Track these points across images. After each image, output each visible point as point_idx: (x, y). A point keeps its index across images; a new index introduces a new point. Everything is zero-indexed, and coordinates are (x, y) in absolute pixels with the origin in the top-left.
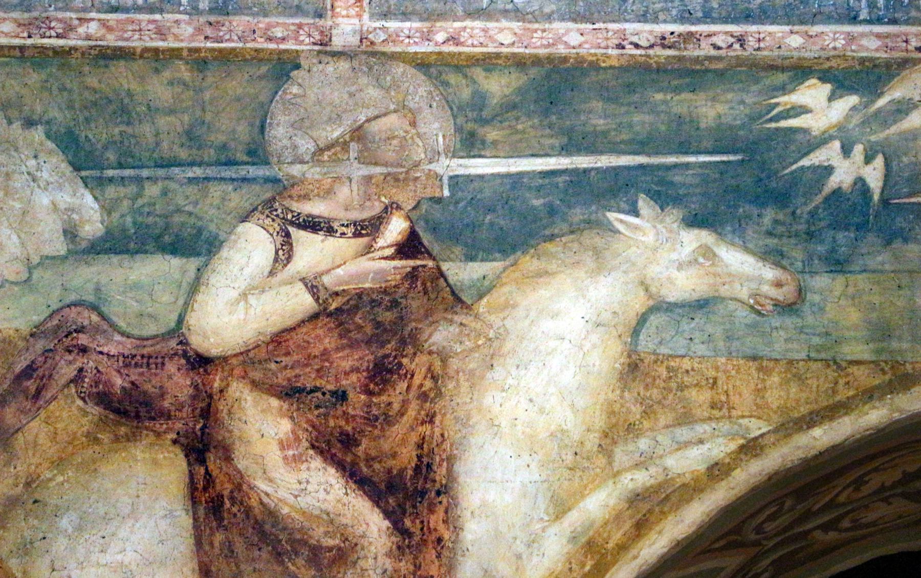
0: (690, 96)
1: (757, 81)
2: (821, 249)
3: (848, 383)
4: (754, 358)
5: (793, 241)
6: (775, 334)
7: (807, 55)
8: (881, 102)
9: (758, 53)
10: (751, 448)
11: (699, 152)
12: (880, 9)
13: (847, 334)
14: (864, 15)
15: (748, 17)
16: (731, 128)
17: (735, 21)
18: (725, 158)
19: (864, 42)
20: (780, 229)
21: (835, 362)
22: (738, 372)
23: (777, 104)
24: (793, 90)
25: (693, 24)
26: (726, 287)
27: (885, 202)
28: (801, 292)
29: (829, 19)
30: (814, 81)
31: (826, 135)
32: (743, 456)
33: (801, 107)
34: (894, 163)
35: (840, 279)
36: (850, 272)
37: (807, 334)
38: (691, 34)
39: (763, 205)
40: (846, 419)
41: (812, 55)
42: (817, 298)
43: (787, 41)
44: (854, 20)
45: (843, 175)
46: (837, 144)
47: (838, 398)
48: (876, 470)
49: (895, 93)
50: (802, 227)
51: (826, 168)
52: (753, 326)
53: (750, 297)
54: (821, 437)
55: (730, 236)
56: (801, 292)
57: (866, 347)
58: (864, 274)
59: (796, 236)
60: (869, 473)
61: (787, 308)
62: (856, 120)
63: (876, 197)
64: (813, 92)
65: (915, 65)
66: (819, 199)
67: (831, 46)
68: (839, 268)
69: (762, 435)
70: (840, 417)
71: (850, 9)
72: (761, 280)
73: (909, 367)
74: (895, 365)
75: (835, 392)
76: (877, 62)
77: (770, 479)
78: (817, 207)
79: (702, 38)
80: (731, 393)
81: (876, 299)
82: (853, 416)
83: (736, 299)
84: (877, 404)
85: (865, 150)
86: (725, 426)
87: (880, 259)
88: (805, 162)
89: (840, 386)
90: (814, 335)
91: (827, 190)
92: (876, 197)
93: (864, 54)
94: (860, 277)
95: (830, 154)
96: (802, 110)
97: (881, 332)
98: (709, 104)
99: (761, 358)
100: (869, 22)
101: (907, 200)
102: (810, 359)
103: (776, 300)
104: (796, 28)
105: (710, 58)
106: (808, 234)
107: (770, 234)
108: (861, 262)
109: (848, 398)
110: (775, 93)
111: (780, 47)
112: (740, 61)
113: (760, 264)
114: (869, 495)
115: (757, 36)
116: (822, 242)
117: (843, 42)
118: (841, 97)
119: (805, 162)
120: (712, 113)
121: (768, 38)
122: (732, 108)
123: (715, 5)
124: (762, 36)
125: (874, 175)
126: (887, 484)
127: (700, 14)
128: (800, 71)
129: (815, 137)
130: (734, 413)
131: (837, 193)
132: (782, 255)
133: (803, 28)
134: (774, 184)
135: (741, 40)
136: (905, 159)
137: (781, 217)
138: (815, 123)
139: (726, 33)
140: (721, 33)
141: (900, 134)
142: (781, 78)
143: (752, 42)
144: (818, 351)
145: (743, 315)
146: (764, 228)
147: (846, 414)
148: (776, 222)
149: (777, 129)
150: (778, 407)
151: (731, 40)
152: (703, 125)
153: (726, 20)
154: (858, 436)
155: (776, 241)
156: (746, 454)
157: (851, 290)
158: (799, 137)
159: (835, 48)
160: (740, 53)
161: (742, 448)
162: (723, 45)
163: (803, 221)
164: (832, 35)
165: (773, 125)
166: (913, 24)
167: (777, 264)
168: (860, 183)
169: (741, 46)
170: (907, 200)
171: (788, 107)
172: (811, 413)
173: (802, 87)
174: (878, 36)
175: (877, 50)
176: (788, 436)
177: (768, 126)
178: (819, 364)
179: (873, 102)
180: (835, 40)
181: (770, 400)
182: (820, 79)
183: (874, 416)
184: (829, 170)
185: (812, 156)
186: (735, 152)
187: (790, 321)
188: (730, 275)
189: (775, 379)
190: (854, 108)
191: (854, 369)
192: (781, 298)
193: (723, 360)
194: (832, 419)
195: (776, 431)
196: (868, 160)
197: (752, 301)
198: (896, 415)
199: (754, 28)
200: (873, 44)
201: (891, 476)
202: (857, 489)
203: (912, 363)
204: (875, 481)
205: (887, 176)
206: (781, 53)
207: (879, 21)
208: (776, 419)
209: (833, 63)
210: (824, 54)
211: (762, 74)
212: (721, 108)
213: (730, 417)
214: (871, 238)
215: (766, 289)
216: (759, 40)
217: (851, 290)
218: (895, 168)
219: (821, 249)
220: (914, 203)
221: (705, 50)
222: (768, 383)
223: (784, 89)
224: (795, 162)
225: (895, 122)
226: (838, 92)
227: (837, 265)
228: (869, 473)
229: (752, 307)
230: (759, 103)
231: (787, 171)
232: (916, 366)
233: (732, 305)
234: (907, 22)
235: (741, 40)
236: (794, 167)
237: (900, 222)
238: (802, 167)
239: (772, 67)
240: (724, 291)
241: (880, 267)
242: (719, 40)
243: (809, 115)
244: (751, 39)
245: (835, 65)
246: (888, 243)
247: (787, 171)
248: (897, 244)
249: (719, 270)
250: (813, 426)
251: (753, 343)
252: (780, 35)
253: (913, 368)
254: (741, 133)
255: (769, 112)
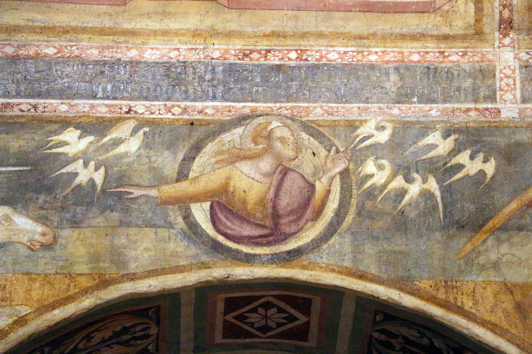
0: (6, 136)
1: (42, 128)
2: (68, 216)
3: (75, 285)
4: (27, 274)
5: (53, 211)
6: (39, 260)
7: (68, 115)
8: (106, 140)
9: (44, 114)
10: (21, 321)
11: (8, 165)
12: (108, 92)
13: (78, 260)
14: (100, 95)
15: (39, 95)
16: (26, 152)
17: (32, 97)
18: (21, 168)
19: (99, 109)
20: (47, 205)
21: (70, 275)
22: (18, 281)
23: (52, 141)
24: (60, 134)
25: (10, 98)
26: (16, 236)
27: (103, 191)
28: (55, 239)
29: (82, 97)
30: (72, 128)
31: (76, 157)
32: (15, 326)
33: (64, 142)
34: (110, 171)
35: (77, 231)
36: (82, 227)
37: (57, 260)
38: (9, 104)
39: (41, 193)
40: (73, 304)
41: (71, 115)
42: (63, 241)
43: (59, 108)
44: (95, 97)
45: (83, 178)
46: (81, 161)
47: (69, 294)
48: (96, 330)
49: (114, 134)
50: (59, 204)
51: (74, 173)
52: (29, 256)
53: (28, 241)
54: (59, 314)
55: (20, 210)
56: (55, 239)
57: (87, 266)
58: (89, 229)
59: (55, 209)
60: (93, 332)
61: (47, 247)
62: (91, 149)
63: (99, 189)
64: (71, 134)
65: (124, 120)
66: (70, 189)
67: (82, 111)
68: (76, 225)
69: (27, 315)
70: (69, 303)
71: (93, 91)
72: (34, 233)
73: (107, 276)
74: (101, 275)
75: (68, 290)
76: (105, 119)
77: (29, 337)
78: (68, 194)
79: (14, 106)
80: (12, 293)
81: (94, 241)
82: (76, 303)
83: (20, 243)
84: (89, 296)
85: (96, 164)
86: (7, 310)
87: (98, 220)
88: (64, 171)
89: (71, 288)
90: (60, 260)
91: (73, 185)
92: (99, 189)
93: (99, 115)
94: (86, 230)
95: (77, 166)
96: (65, 143)
97: (95, 258)
98: (15, 140)
99: (31, 274)
100: (102, 98)
101: (114, 190)
102: (57, 273)
103: (42, 243)
104: (65, 101)
105: (18, 117)
106: (61, 208)
107: (42, 208)
108: (88, 222)
109: (75, 294)
110: (51, 135)
111: (55, 111)
112: (34, 118)
113: (35, 224)
114: (99, 343)
115: (44, 105)
116: (68, 212)
117: (88, 109)
118: (85, 137)
119: (64, 171)
120: (16, 145)
121: (49, 106)
122: (28, 143)
123: (23, 89)
124: (46, 105)
125: (99, 177)
126: (106, 337)
127: (14, 93)
128: (65, 123)
129: (70, 158)
130: (13, 303)
131: (79, 186)
132: (47, 219)
133: (69, 101)
134: (46, 182)
135: (35, 107)
136: (115, 169)
137: (48, 199)
138: (70, 150)
139: (27, 103)
140: (25, 103)
141: (114, 156)
142: (55, 127)
143: (41, 108)
144: (62, 269)
145: (24, 251)
146: (38, 206)
147: (73, 302)
148: (45, 202)
149: (50, 154)
150: (37, 300)
151: (30, 107)
152: (11, 152)
153: (27, 97)
154: (78, 313)
155: (45, 212)
156: (17, 325)
157: (82, 237)
158: (62, 157)
159: (84, 112)
160: (33, 114)
161: (15, 322)
162: (26, 110)
163: (59, 201)
164: (83, 105)
165: (49, 151)
166: (125, 100)
167: (44, 224)
168: (92, 181)
169: (35, 110)
170: (114, 190)
171: (57, 142)
172: (55, 302)
173: (65, 131)
174: (107, 106)
175: (106, 113)
176: (41, 314)
177: (45, 152)
178: (62, 276)
179: (102, 139)
180: (84, 107)
181: (33, 296)
182: (74, 127)
183: (87, 303)
184: (76, 174)
185: (67, 167)
186: (27, 165)
187: (47, 254)
188: (18, 230)
189: (38, 284)
190: (91, 143)
191: (79, 279)
192: (45, 242)
193: (10, 275)
194: (65, 304)
195: (35, 312)
196: (97, 169)
197: (29, 244)
198: (99, 302)
199: (42, 101)
200: (104, 109)
201: (108, 334)
202: (88, 341)
203: (109, 274)
204: (98, 337)
205: (105, 178)
206: (56, 114)
207: (108, 98)
208: (36, 305)
209: (83, 119)
210: (78, 115)
211: (45, 125)
212: (22, 143)
213: (11, 305)
214: (95, 210)
215: (38, 237)
216: (45, 107)
217: (82, 237)
218: (110, 173)
219: (68, 216)
220: (118, 192)
221: (16, 112)
222: (34, 286)
223: (56, 133)
224: (58, 170)
225: (112, 150)
226: (84, 134)
227: (75, 224)
228: (93, 332)
229: (29, 247)
230: (42, 140)
231: (53, 175)
232: (111, 275)
233: (19, 246)
234: (123, 99)
235: (35, 107)
236: (58, 173)
237: (110, 202)
238: (62, 173)
239: (50, 121)
240: (15, 239)
241: (97, 225)
242: (24, 107)
243: (68, 146)
244: (40, 106)
245: (83, 120)
246: (103, 212)
247: (53, 175)
248: (108, 212)
249: (13, 227)
250: (55, 309)
251: (29, 266)
252: (56, 105)
253: (110, 277)
254: (31, 155)
255: (47, 144)
